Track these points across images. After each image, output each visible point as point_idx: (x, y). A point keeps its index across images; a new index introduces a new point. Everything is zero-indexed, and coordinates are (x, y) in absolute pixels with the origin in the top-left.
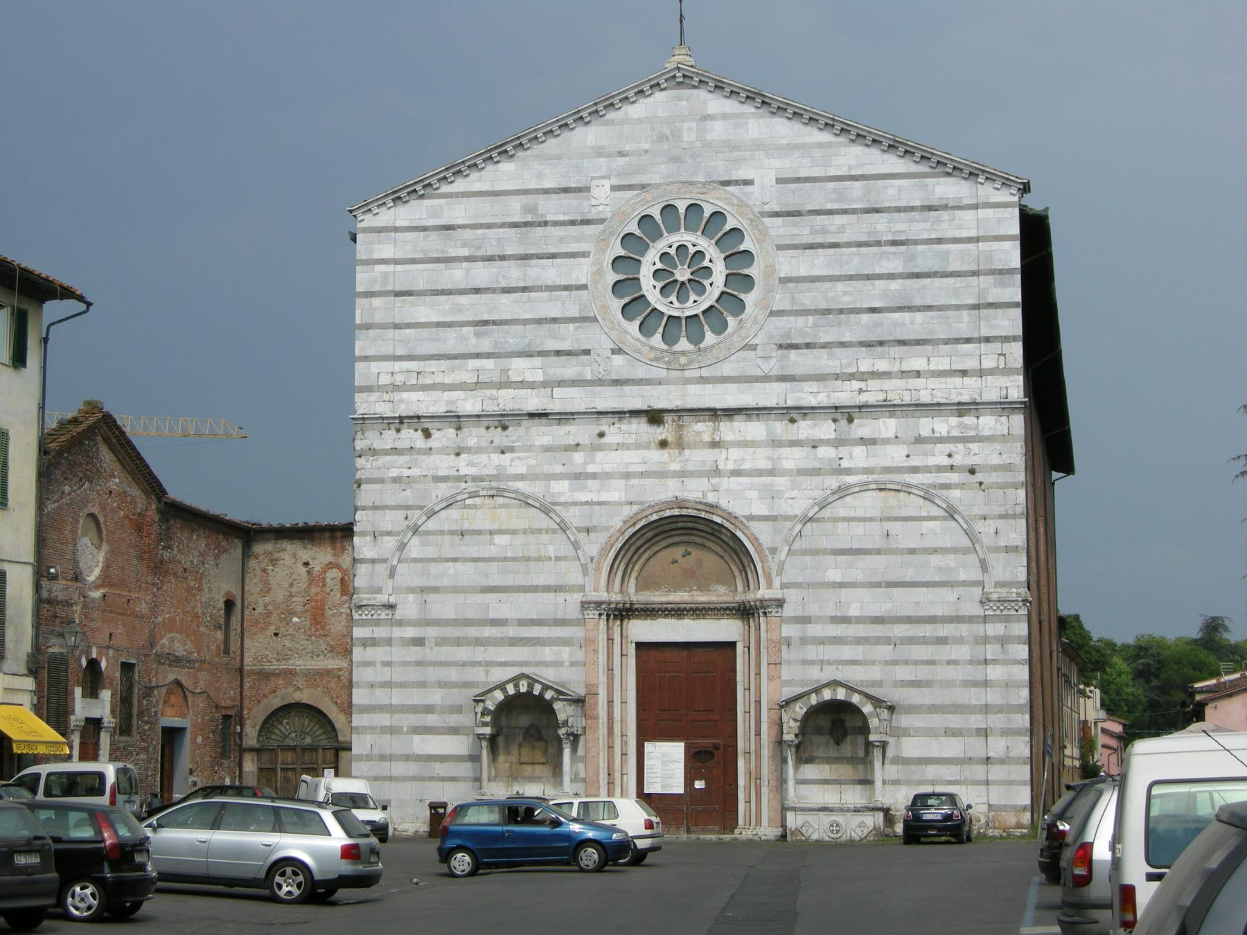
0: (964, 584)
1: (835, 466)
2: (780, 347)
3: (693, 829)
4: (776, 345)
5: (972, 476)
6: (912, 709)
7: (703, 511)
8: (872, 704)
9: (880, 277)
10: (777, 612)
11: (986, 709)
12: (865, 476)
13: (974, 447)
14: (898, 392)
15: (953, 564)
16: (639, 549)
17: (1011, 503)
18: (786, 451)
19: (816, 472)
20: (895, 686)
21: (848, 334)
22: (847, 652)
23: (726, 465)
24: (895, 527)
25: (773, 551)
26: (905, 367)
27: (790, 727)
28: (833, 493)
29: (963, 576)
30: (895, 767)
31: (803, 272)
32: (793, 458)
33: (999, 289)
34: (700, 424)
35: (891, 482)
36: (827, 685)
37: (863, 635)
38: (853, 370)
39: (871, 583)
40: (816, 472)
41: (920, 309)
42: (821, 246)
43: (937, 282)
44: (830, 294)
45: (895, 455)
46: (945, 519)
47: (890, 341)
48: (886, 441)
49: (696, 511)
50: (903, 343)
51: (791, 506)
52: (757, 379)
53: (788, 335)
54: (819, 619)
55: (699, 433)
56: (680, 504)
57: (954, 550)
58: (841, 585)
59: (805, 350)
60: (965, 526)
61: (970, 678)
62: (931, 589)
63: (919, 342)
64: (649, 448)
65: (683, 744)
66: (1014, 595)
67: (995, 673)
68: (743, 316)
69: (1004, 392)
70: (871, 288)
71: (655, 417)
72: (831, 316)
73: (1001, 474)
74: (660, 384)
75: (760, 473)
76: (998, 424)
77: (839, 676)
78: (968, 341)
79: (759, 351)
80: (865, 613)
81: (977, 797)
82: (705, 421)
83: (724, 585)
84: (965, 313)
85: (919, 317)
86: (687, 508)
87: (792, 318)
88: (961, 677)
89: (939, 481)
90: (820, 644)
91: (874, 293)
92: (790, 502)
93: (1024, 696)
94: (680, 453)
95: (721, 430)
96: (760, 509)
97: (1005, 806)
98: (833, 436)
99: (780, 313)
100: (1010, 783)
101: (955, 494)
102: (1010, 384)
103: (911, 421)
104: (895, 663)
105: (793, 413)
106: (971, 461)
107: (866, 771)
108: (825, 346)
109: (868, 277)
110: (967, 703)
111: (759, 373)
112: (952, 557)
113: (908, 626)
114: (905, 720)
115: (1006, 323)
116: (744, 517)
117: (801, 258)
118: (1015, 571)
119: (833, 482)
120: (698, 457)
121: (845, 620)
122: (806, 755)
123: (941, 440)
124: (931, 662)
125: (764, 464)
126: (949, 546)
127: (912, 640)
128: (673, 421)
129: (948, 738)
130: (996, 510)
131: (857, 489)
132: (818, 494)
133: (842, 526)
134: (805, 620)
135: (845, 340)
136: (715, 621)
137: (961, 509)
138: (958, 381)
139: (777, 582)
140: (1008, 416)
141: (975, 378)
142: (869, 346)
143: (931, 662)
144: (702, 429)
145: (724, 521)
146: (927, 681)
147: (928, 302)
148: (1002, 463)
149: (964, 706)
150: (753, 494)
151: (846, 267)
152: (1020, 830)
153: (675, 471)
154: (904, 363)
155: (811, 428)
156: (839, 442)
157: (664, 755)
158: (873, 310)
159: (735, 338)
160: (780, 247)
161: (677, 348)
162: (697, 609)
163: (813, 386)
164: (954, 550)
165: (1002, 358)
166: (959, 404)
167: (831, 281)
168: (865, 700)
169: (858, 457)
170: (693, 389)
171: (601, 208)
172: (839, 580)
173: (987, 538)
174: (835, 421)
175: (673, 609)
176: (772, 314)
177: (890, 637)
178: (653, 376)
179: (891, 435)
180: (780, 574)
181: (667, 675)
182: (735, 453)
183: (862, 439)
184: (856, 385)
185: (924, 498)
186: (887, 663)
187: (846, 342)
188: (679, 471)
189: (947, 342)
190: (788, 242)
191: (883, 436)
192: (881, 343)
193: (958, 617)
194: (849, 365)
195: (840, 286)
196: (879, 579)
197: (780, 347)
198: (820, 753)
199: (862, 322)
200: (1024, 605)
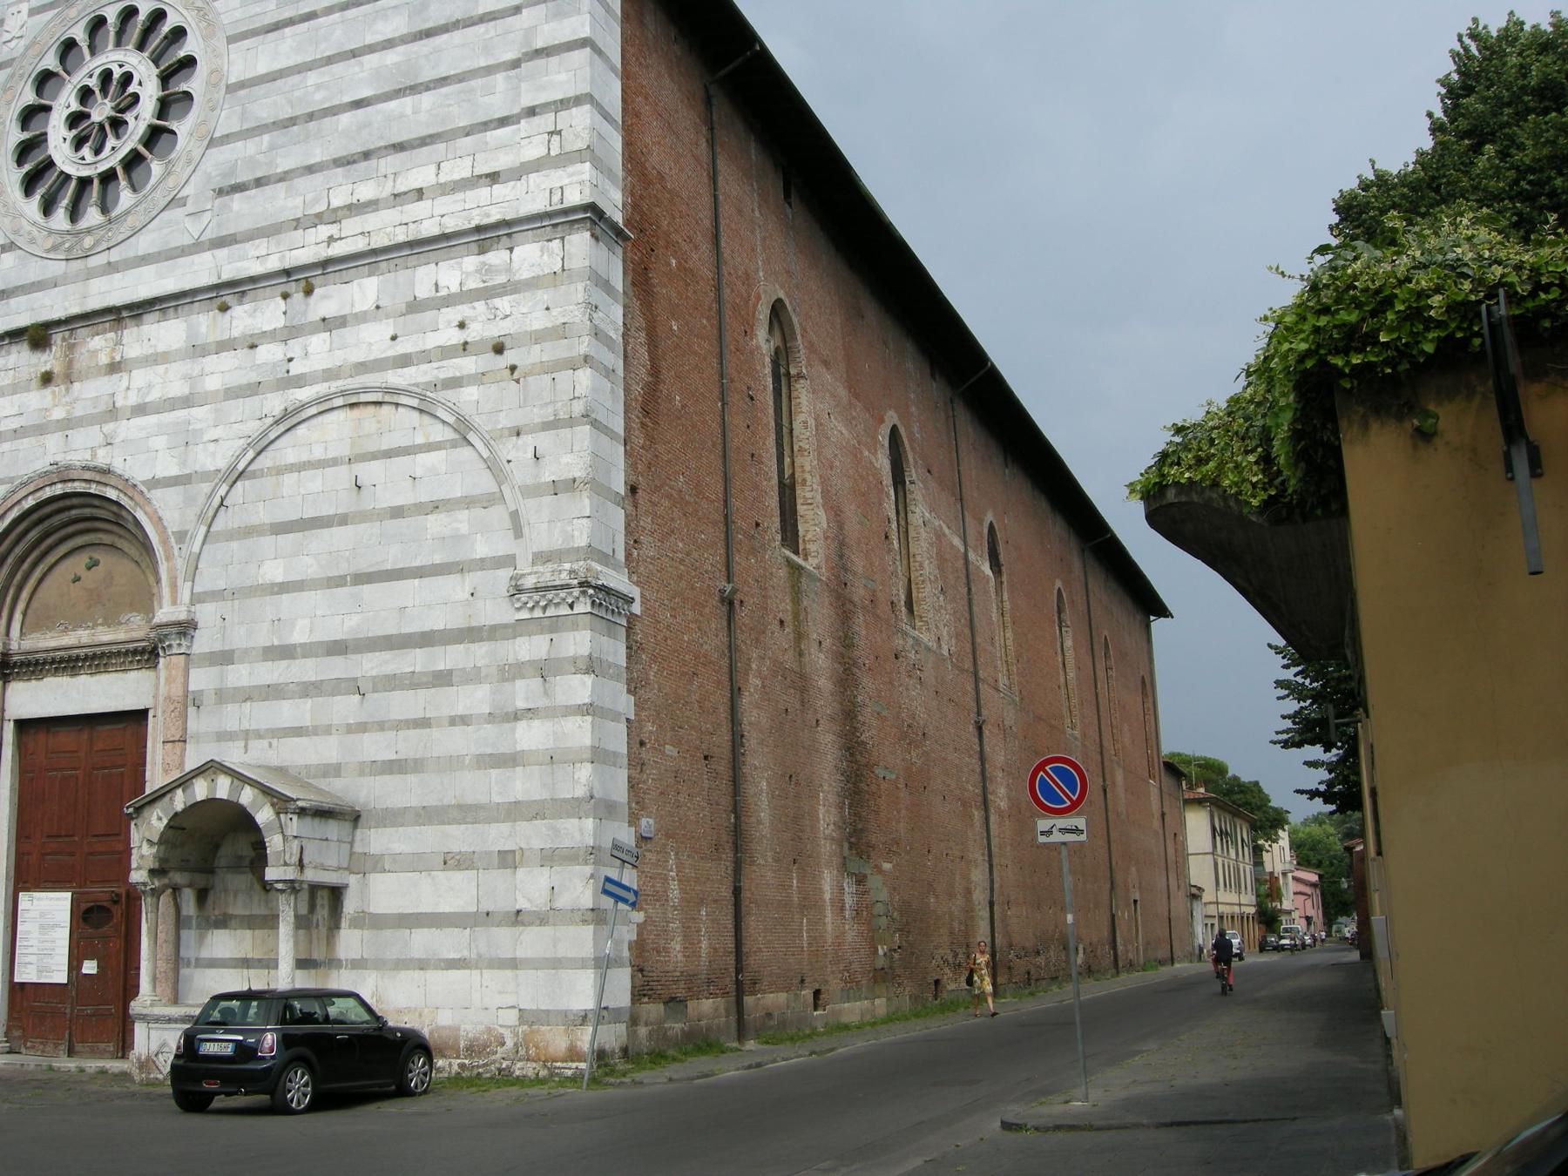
0: (482, 564)
1: (282, 374)
2: (221, 192)
3: (78, 1047)
4: (214, 190)
5: (498, 357)
6: (392, 818)
7: (94, 481)
8: (273, 805)
9: (371, 49)
10: (180, 645)
11: (515, 811)
12: (326, 385)
13: (503, 304)
14: (388, 230)
15: (464, 529)
16: (22, 560)
17: (566, 397)
18: (211, 362)
19: (253, 389)
20: (362, 774)
21: (318, 151)
22: (289, 712)
23: (126, 398)
24: (370, 472)
25: (182, 536)
26: (401, 188)
27: (142, 857)
28: (277, 423)
29: (482, 550)
30: (357, 933)
31: (262, 68)
32: (221, 371)
33: (553, 25)
34: (97, 338)
35: (366, 390)
36: (200, 772)
37: (313, 679)
38: (322, 207)
39: (329, 579)
40: (253, 389)
41: (428, 87)
42: (291, 22)
43: (457, 36)
44: (297, 94)
45: (373, 340)
46: (454, 444)
47: (380, 148)
48: (362, 318)
49: (83, 485)
50: (399, 147)
51: (213, 454)
52: (183, 251)
53: (232, 171)
54: (246, 655)
55: (95, 353)
56: (62, 473)
57: (468, 502)
58: (283, 588)
59: (254, 191)
60: (486, 454)
61: (489, 751)
62: (426, 581)
63: (424, 141)
64: (28, 390)
65: (66, 896)
66: (564, 575)
67: (531, 736)
68: (173, 156)
69: (556, 198)
70: (357, 69)
71: (37, 336)
72: (295, 128)
73: (548, 345)
74: (56, 286)
75: (172, 404)
76: (545, 257)
77: (233, 756)
78: (503, 122)
79: (190, 208)
80: (319, 636)
81: (500, 993)
82: (104, 332)
83: (139, 612)
84: (500, 78)
85: (427, 99)
86: (74, 480)
87: (240, 144)
88: (474, 750)
89: (443, 375)
90: (245, 701)
91: (359, 78)
92: (212, 447)
93: (583, 780)
94: (67, 390)
95: (124, 342)
96: (168, 467)
97: (547, 1012)
98: (280, 322)
99: (227, 139)
100: (556, 964)
101: (470, 393)
102: (566, 181)
103: (402, 275)
104: (362, 728)
105: (226, 293)
106: (495, 331)
107: (311, 942)
108: (284, 177)
109: (354, 54)
110: (482, 799)
111: (187, 240)
112: (463, 515)
113: (386, 655)
114: (375, 840)
115: (563, 77)
116: (144, 483)
117: (260, 48)
118: (569, 528)
119: (275, 404)
120: (91, 392)
121: (285, 652)
122: (217, 912)
123: (450, 301)
124: (423, 723)
125: (178, 389)
126: (459, 495)
127: (392, 683)
128: (64, 339)
129: (450, 874)
130: (539, 415)
131: (314, 410)
132: (253, 427)
133: (290, 479)
134: (224, 658)
135: (312, 162)
136: (120, 675)
137: (477, 420)
138: (483, 193)
139: (185, 595)
140: (563, 239)
141: (512, 183)
142: (349, 163)
143: (423, 723)
144: (98, 345)
145: (122, 495)
146: (415, 761)
147: (443, 71)
148: (550, 325)
149: (477, 807)
150: (160, 442)
151: (323, 46)
152: (574, 1065)
153: (58, 421)
154: (398, 182)
155: (250, 316)
156: (291, 332)
157: (43, 914)
158: (358, 104)
159: (158, 194)
160: (231, 40)
161: (84, 224)
162: (94, 656)
163: (260, 246)
164: (468, 502)
165: (556, 138)
166: (479, 229)
167: (299, 72)
168: (261, 797)
169: (317, 352)
170: (97, 284)
171: (12, 44)
172: (280, 579)
173: (521, 473)
174: (285, 296)
175: (62, 660)
176: (212, 143)
177: (355, 679)
178: (48, 275)
179: (367, 305)
180: (192, 577)
181: (59, 774)
182: (140, 377)
183: (324, 320)
184: (324, 231)
185: (421, 411)
186: (351, 729)
187: (313, 165)
188: (64, 419)
189: (468, 132)
190: (246, 29)
191: (357, 309)
192: (366, 155)
193: (471, 630)
194: (316, 201)
195: (312, 78)
196: (343, 569)
197: (221, 192)
198: (238, 909)
199: (340, 128)
200: (584, 593)
